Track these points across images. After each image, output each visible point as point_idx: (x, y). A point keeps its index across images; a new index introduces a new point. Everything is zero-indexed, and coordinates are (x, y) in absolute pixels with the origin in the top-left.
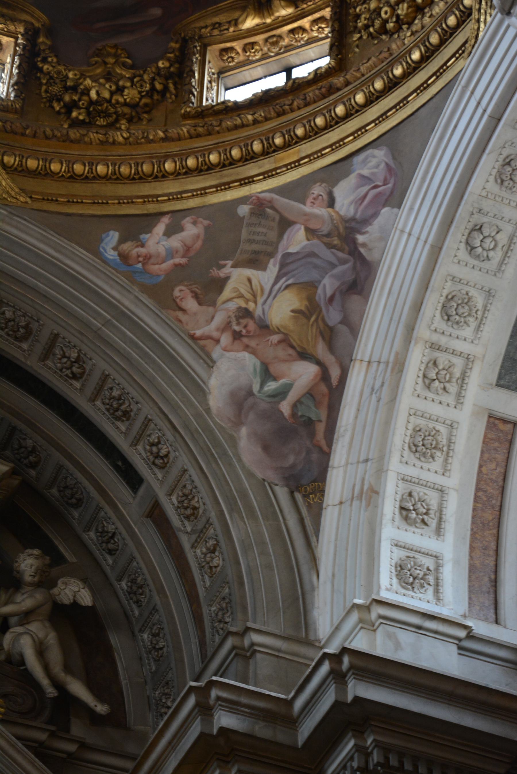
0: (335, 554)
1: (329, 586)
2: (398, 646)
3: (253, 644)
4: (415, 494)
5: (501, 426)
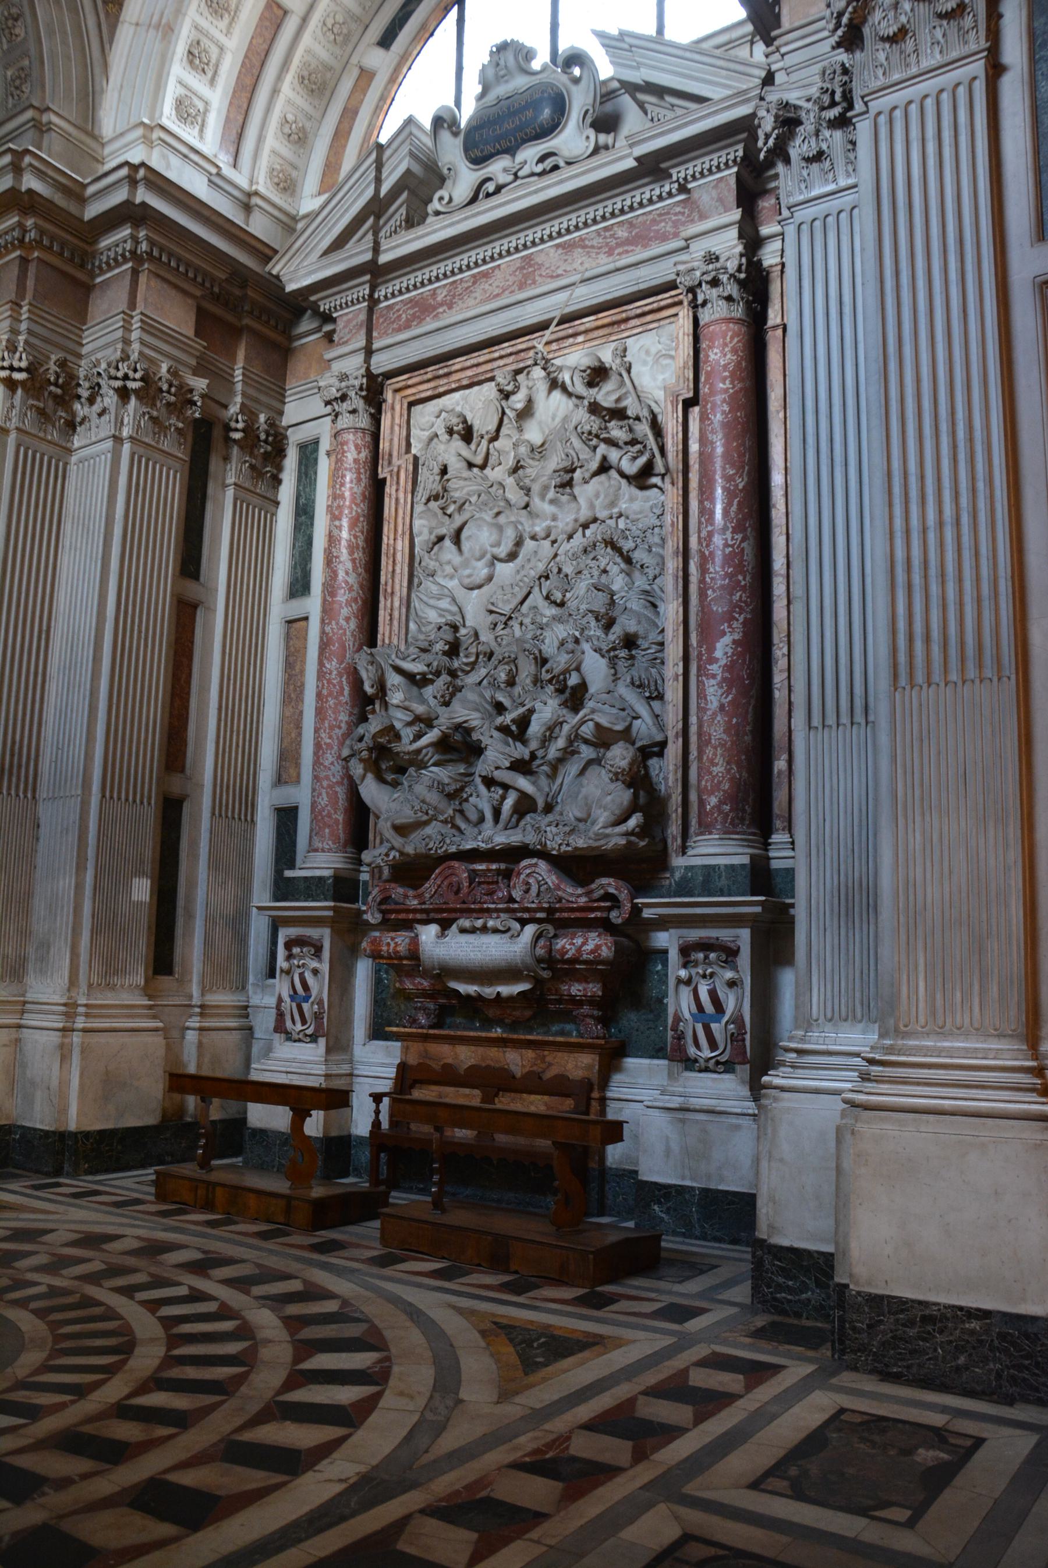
0: (125, 69)
1: (116, 95)
2: (168, 166)
3: (50, 123)
4: (202, 44)
5: (275, 9)
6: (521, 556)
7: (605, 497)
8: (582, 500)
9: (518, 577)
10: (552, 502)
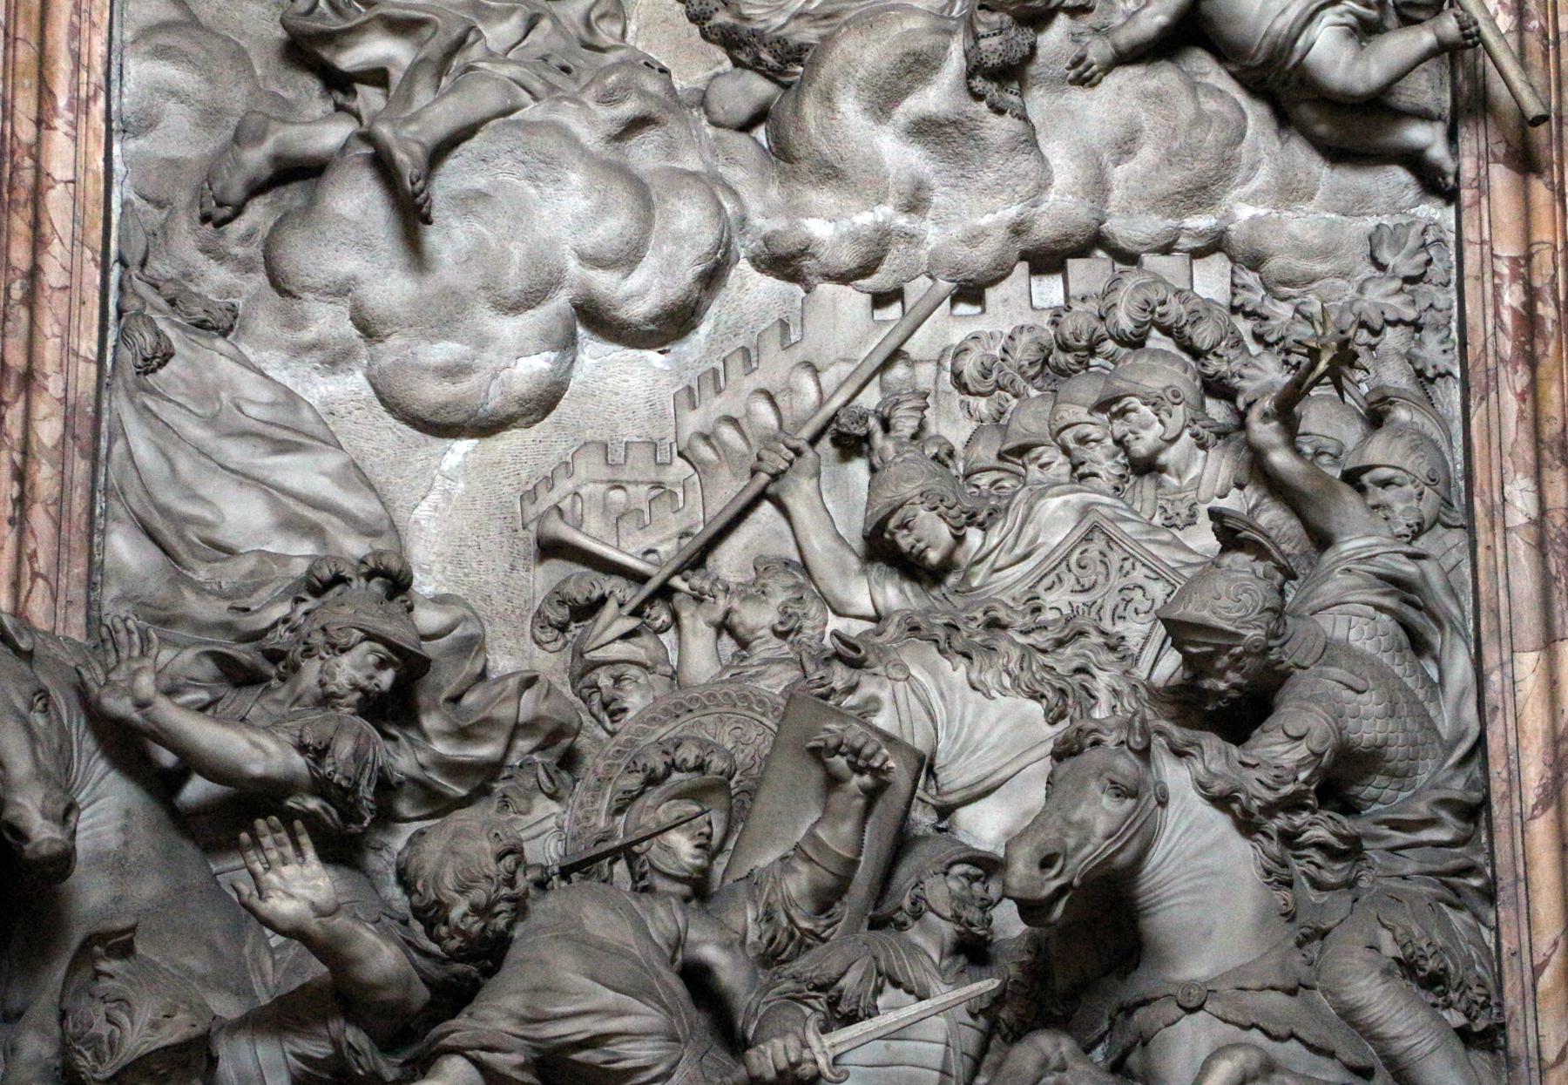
6: (705, 328)
7: (1171, 158)
8: (1056, 151)
9: (693, 421)
10: (925, 130)
